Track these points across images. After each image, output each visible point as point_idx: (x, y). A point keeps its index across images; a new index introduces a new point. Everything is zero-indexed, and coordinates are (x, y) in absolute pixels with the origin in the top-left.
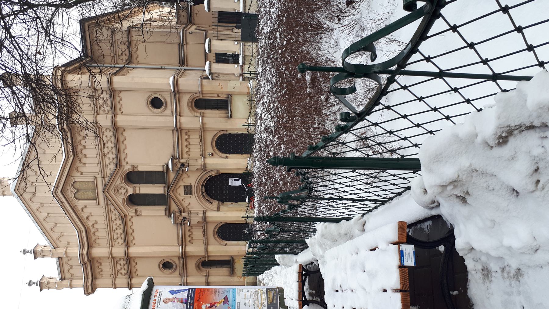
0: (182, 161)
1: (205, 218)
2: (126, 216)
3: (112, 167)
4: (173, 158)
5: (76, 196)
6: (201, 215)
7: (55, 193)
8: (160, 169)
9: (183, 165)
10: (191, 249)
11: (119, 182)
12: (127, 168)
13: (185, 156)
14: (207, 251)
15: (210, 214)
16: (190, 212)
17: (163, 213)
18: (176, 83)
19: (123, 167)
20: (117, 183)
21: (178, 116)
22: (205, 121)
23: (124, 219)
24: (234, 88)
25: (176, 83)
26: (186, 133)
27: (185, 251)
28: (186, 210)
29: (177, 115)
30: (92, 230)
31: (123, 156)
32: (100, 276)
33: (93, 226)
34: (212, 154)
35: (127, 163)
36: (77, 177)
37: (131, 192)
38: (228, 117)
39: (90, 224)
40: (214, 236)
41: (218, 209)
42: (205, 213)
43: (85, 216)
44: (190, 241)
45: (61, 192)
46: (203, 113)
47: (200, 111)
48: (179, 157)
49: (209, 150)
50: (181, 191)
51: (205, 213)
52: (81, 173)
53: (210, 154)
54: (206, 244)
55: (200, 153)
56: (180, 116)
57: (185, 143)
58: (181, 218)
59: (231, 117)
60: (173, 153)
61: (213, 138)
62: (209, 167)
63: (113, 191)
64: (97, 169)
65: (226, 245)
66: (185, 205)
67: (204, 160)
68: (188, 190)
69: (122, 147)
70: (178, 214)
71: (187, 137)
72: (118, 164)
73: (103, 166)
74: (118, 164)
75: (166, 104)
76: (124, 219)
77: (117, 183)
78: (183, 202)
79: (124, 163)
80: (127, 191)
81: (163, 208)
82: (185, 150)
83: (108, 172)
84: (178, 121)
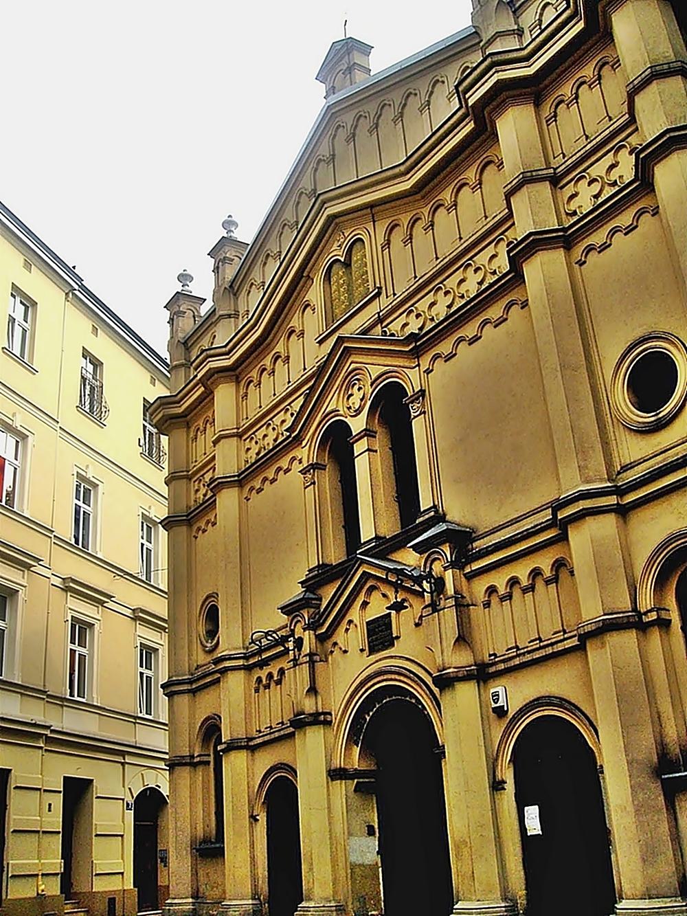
0: (449, 575)
2: (298, 441)
3: (414, 327)
6: (309, 706)
7: (324, 203)
8: (425, 502)
9: (439, 584)
10: (236, 683)
11: (375, 371)
12: (412, 379)
13: (479, 587)
14: (233, 746)
15: (314, 738)
21: (613, 500)
26: (559, 565)
28: (329, 644)
29: (620, 492)
30: (267, 361)
32: (192, 435)
33: (277, 358)
34: (500, 712)
35: (428, 372)
37: (357, 424)
39: (280, 348)
41: (336, 774)
42: (320, 719)
43: (295, 322)
44: (259, 680)
45: (332, 218)
46: (664, 624)
47: (671, 602)
48: (469, 562)
49: (515, 693)
50: (378, 607)
52: (388, 243)
53: (496, 696)
54: (249, 746)
55: (501, 651)
57: (522, 571)
61: (563, 703)
62: (446, 699)
63: (353, 366)
65: (254, 818)
66: (340, 637)
67: (467, 678)
68: (380, 635)
71: (548, 573)
72: (418, 345)
74: (418, 345)
78: (344, 625)
79: (425, 362)
80: (358, 412)
81: (335, 555)
82: (500, 580)
83: (395, 327)
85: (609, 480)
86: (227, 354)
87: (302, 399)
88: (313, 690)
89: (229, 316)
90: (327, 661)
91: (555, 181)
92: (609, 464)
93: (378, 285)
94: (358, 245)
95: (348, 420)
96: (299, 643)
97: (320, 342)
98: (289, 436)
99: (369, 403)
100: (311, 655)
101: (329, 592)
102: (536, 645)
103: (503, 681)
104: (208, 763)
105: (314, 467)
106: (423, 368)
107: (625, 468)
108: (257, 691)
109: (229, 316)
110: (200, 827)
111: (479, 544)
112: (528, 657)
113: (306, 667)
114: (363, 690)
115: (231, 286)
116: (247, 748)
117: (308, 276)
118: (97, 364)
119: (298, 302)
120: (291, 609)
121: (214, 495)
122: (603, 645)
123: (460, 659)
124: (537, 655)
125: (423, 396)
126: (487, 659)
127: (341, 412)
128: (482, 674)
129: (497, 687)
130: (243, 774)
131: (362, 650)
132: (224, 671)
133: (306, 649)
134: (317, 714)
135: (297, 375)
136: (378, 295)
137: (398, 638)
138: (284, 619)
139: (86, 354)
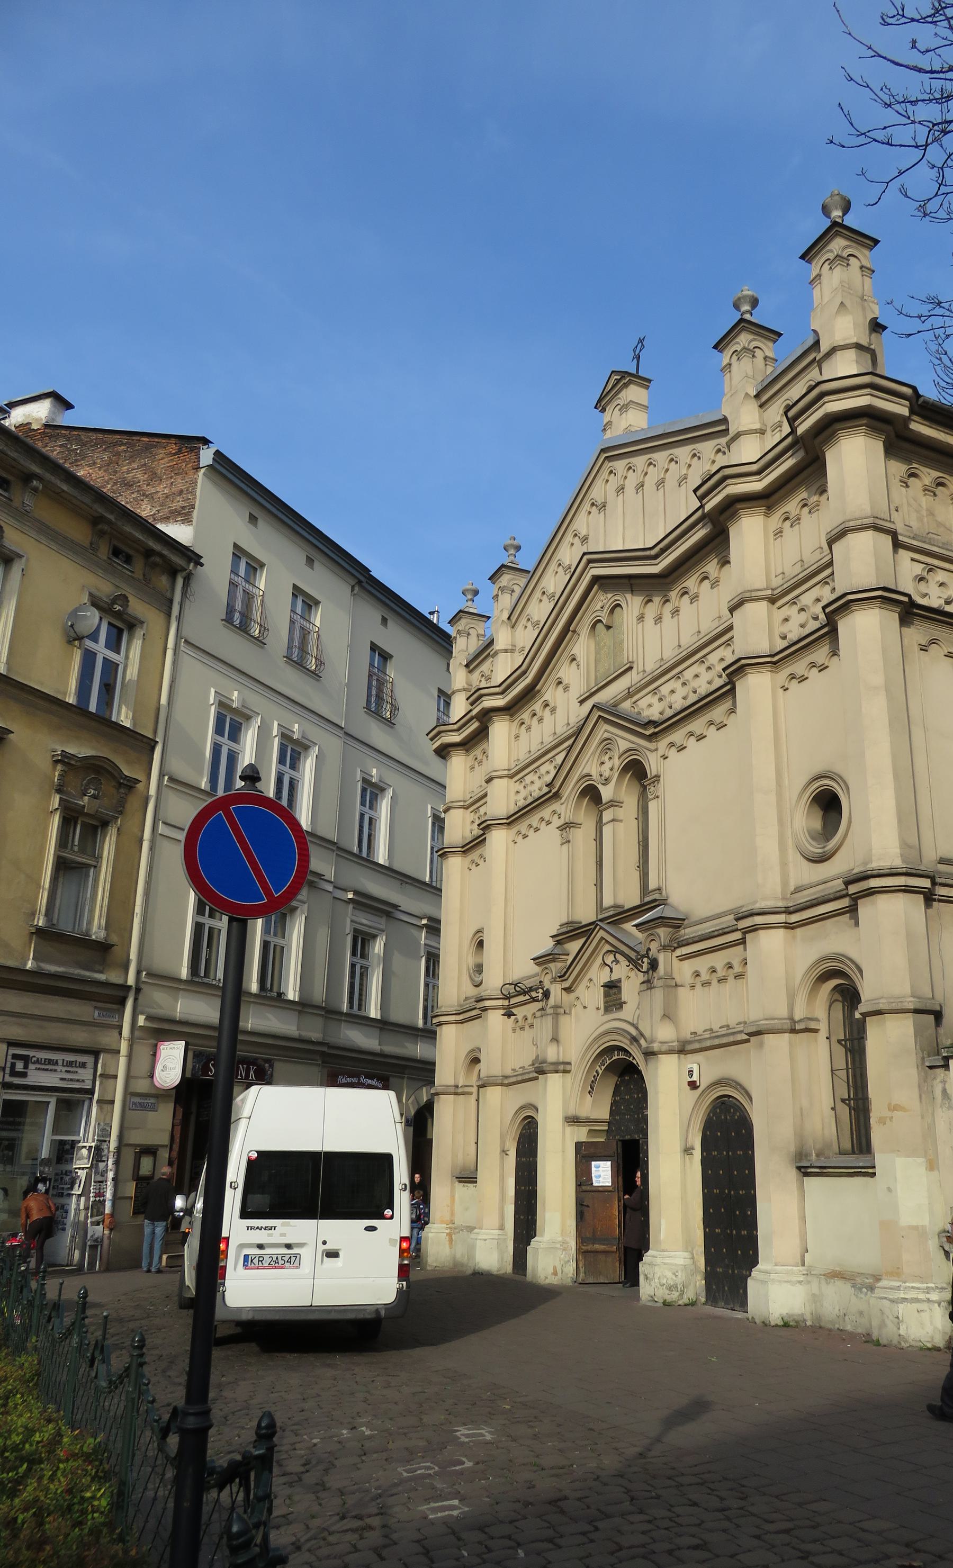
0: (661, 958)
1: (540, 1069)
2: (557, 796)
4: (676, 923)
5: (599, 625)
6: (552, 1053)
9: (654, 965)
11: (623, 745)
16: (558, 1012)
17: (565, 920)
18: (874, 883)
19: (651, 746)
20: (620, 741)
21: (781, 918)
22: (769, 1039)
23: (552, 795)
24: (889, 1190)
25: (874, 883)
27: (485, 1009)
30: (537, 706)
31: (677, 736)
34: (693, 1085)
35: (665, 758)
36: (632, 604)
38: (800, 1155)
40: (522, 1108)
41: (573, 1120)
42: (562, 1068)
51: (562, 1068)
53: (691, 1073)
54: (506, 1082)
56: (789, 926)
58: (547, 985)
59: (804, 1171)
60: (694, 918)
61: (738, 1086)
63: (606, 735)
64: (651, 665)
65: (504, 1152)
66: (581, 990)
67: (670, 1052)
69: (697, 725)
70: (556, 967)
72: (656, 730)
73: (652, 682)
74: (656, 730)
75: (822, 859)
76: (552, 795)
77: (620, 741)
78: (585, 982)
80: (607, 781)
84: (759, 920)
85: (784, 898)
86: (502, 693)
87: (563, 755)
88: (555, 1039)
89: (506, 651)
90: (570, 1014)
91: (772, 600)
92: (785, 883)
93: (631, 660)
94: (618, 609)
95: (600, 787)
96: (547, 995)
97: (581, 702)
98: (550, 791)
99: (617, 774)
100: (556, 1007)
101: (574, 947)
102: (724, 1031)
103: (699, 1057)
104: (471, 1094)
105: (566, 827)
106: (660, 753)
107: (798, 890)
108: (514, 1030)
109: (506, 651)
110: (460, 1156)
111: (688, 932)
112: (717, 1042)
113: (549, 1021)
114: (596, 1046)
115: (509, 618)
116: (502, 1085)
117: (574, 631)
118: (385, 657)
119: (565, 654)
120: (542, 960)
121: (484, 834)
122: (761, 1045)
123: (664, 1033)
124: (725, 1040)
125: (658, 781)
126: (688, 1036)
127: (594, 778)
128: (682, 1050)
129: (692, 1062)
130: (500, 1107)
131: (598, 1009)
132: (485, 1009)
133: (552, 1001)
134: (557, 1063)
135: (562, 730)
136: (631, 668)
137: (625, 1003)
138: (537, 969)
139: (374, 647)
